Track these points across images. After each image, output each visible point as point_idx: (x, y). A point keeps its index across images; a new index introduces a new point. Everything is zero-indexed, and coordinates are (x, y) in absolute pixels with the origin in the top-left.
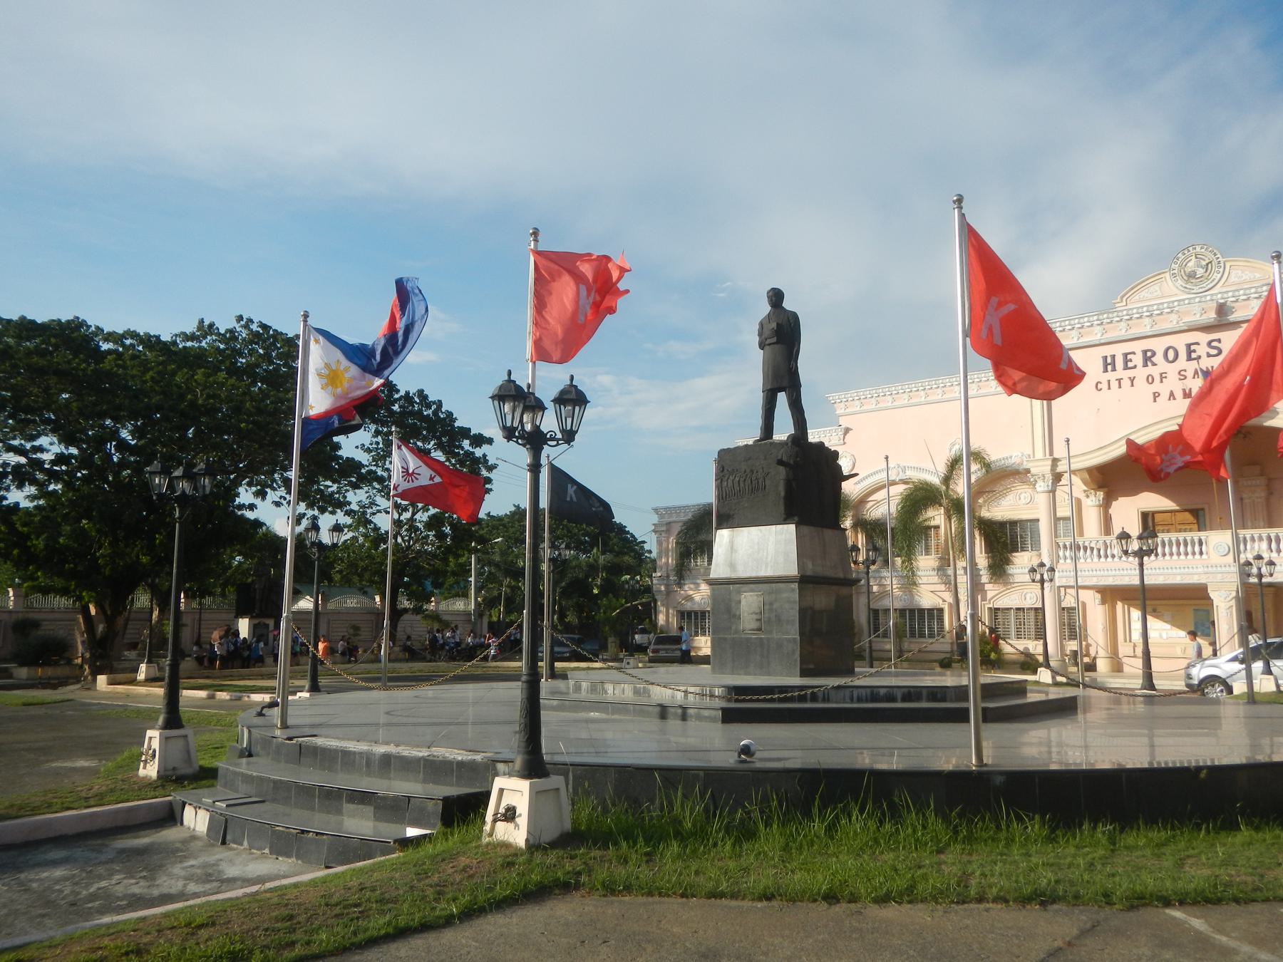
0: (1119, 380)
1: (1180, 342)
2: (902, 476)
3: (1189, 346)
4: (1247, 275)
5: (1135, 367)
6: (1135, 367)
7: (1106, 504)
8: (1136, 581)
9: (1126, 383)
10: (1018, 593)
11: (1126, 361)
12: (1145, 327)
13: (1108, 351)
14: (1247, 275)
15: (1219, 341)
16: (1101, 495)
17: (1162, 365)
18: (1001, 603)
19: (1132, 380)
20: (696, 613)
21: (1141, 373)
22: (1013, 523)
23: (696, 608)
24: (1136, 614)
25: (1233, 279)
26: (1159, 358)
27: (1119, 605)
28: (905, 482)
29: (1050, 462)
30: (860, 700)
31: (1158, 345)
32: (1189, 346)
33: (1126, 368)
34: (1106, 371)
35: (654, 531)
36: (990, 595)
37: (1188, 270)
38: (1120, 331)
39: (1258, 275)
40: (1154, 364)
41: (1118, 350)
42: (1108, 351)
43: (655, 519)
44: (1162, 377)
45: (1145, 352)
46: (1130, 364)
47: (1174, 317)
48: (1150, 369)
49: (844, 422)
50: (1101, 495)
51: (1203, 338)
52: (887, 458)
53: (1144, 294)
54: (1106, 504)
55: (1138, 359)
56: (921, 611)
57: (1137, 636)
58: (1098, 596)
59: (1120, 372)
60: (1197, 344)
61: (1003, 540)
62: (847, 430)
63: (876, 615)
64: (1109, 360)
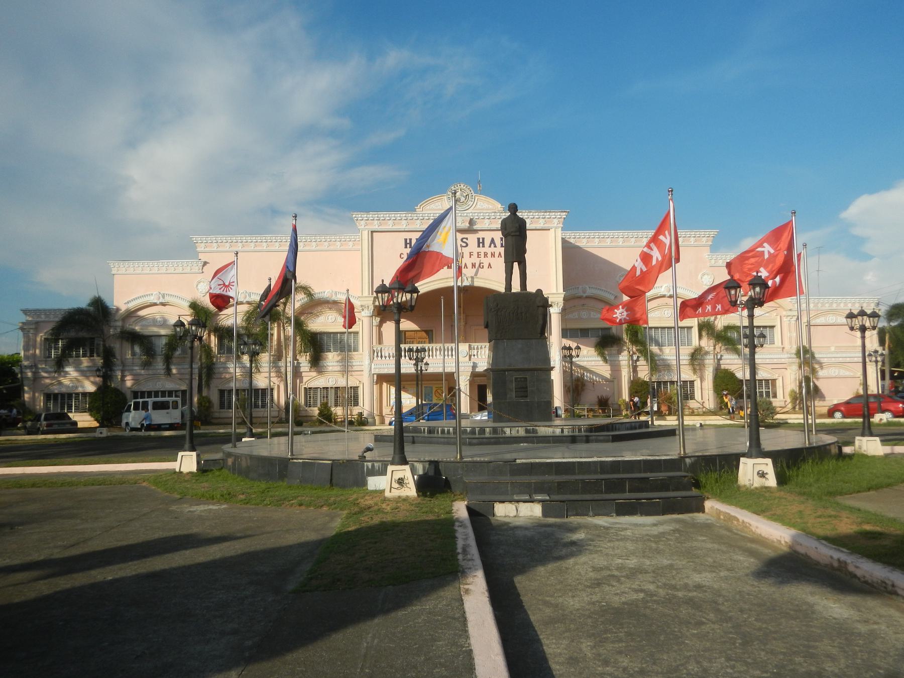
2: (248, 299)
4: (486, 206)
7: (380, 325)
8: (393, 371)
10: (331, 376)
13: (408, 236)
14: (486, 206)
16: (378, 319)
18: (313, 385)
20: (63, 395)
22: (322, 334)
23: (64, 390)
24: (393, 390)
25: (478, 206)
27: (385, 385)
28: (248, 303)
30: (632, 429)
35: (22, 329)
36: (305, 379)
43: (24, 318)
49: (203, 257)
50: (378, 319)
53: (432, 206)
54: (380, 325)
56: (257, 390)
57: (393, 401)
61: (316, 346)
62: (205, 263)
63: (224, 394)
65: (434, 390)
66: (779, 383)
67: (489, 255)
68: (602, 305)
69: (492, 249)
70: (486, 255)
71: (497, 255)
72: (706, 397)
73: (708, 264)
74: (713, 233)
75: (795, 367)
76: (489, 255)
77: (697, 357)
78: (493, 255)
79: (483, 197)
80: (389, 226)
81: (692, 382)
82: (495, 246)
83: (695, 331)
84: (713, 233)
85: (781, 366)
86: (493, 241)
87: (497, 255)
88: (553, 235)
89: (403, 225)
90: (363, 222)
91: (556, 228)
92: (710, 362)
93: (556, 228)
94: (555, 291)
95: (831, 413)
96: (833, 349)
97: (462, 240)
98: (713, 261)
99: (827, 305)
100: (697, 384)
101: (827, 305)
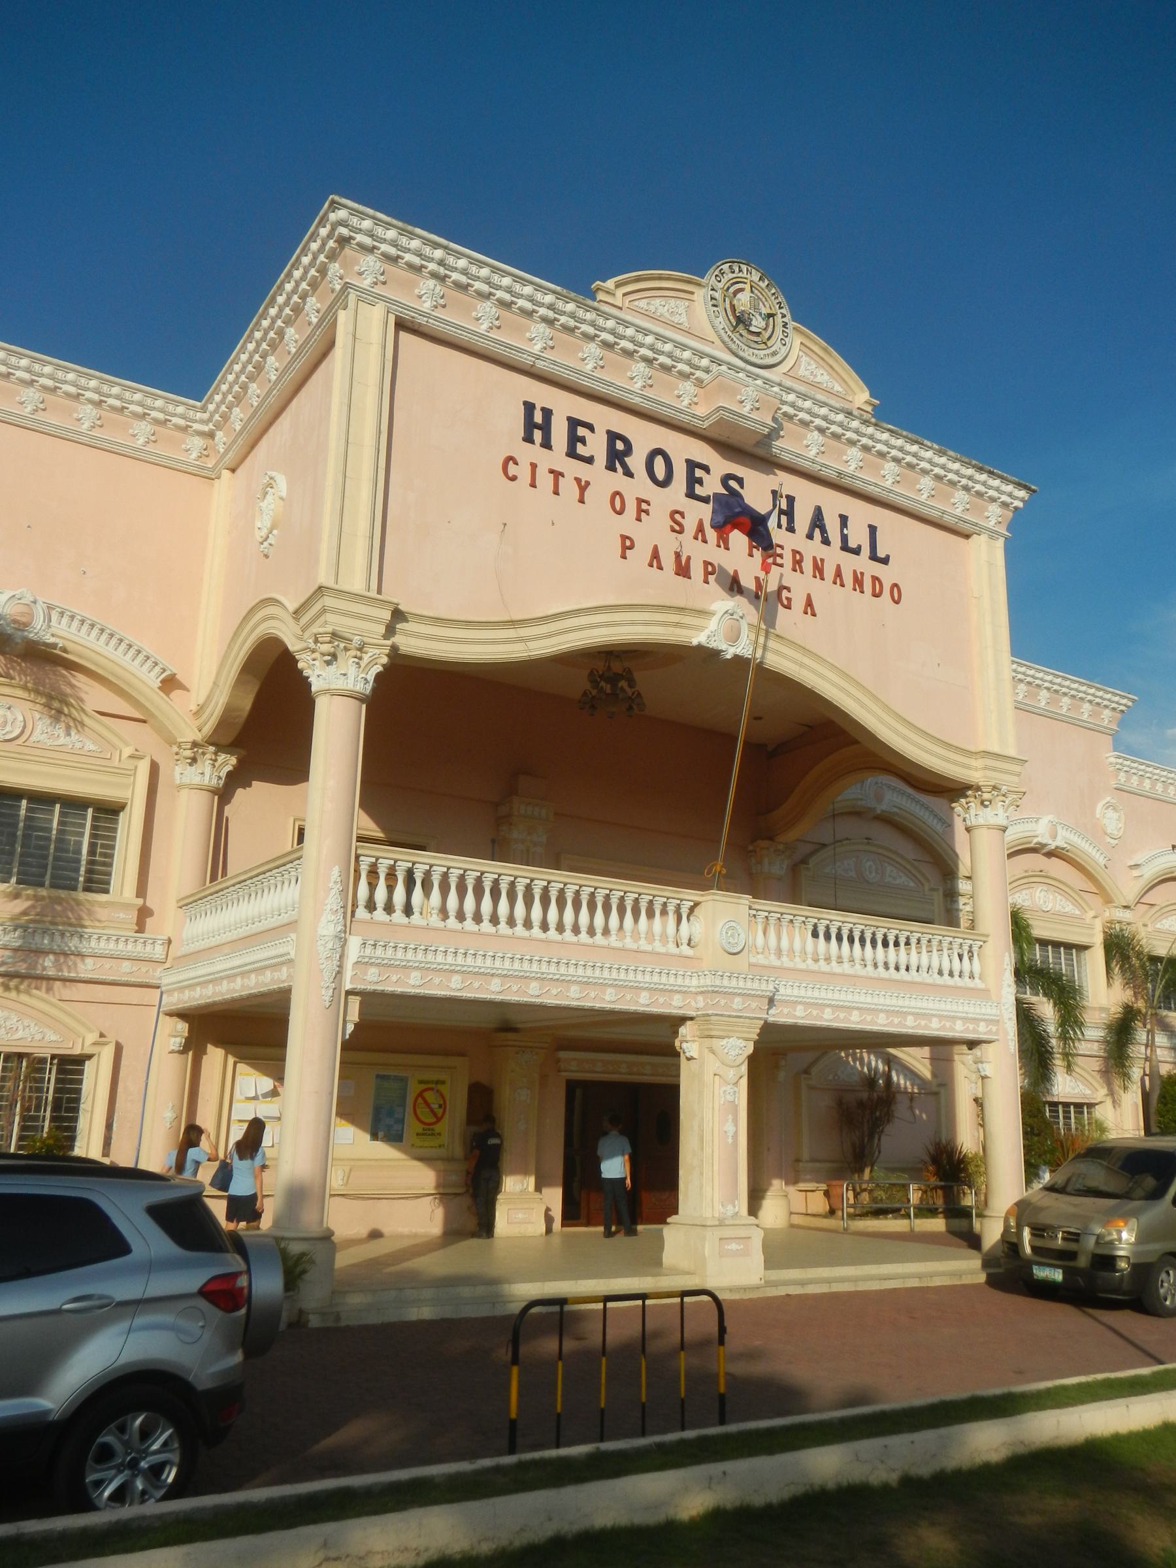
0: (557, 475)
1: (683, 449)
3: (692, 465)
4: (823, 377)
5: (589, 460)
6: (589, 460)
7: (224, 794)
9: (568, 486)
11: (574, 440)
12: (632, 380)
14: (823, 377)
15: (740, 481)
16: (229, 762)
17: (639, 486)
19: (583, 486)
21: (603, 481)
26: (636, 462)
29: (387, 615)
31: (644, 437)
32: (692, 465)
33: (572, 453)
34: (529, 439)
37: (740, 308)
38: (585, 361)
39: (838, 388)
40: (628, 473)
41: (564, 406)
42: (544, 396)
44: (642, 508)
45: (613, 437)
46: (581, 449)
47: (688, 387)
48: (617, 480)
50: (229, 762)
51: (720, 466)
53: (659, 306)
54: (224, 794)
55: (596, 446)
58: (183, 1027)
59: (557, 457)
60: (707, 469)
64: (538, 418)
65: (413, 1089)
67: (808, 565)
68: (908, 850)
69: (813, 549)
70: (797, 564)
71: (829, 572)
73: (1113, 783)
74: (1124, 702)
76: (808, 565)
77: (1121, 1031)
78: (818, 569)
79: (817, 344)
80: (479, 321)
82: (826, 541)
84: (1124, 702)
86: (818, 521)
87: (829, 572)
89: (533, 341)
90: (370, 262)
94: (996, 749)
97: (726, 479)
98: (1122, 777)
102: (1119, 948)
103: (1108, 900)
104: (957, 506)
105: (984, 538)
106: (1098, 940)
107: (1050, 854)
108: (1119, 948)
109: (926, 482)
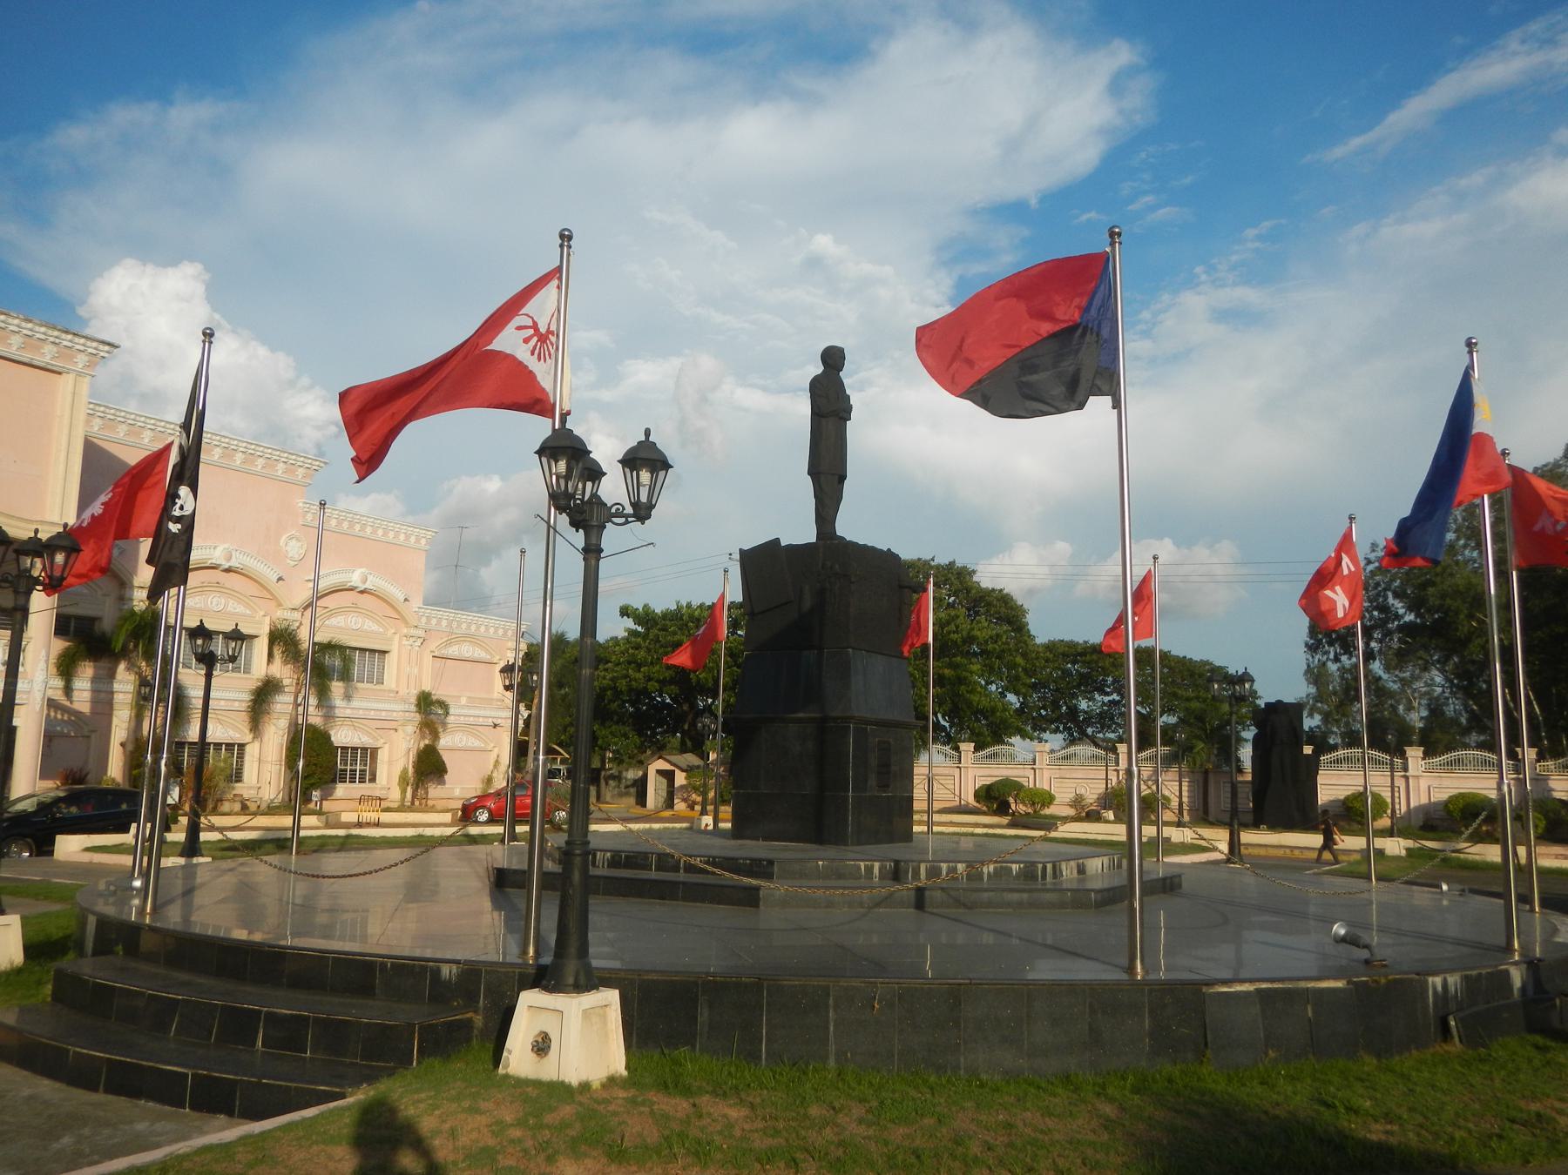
52: (323, 504)
66: (382, 756)
72: (266, 776)
75: (411, 729)
77: (264, 693)
81: (242, 746)
83: (261, 646)
85: (388, 725)
88: (70, 388)
91: (79, 374)
92: (282, 705)
93: (79, 374)
95: (467, 813)
96: (463, 701)
99: (464, 626)
100: (252, 751)
101: (464, 626)
102: (282, 639)
103: (280, 605)
104: (46, 355)
105: (71, 376)
106: (264, 631)
107: (228, 570)
108: (282, 639)
109: (16, 340)
